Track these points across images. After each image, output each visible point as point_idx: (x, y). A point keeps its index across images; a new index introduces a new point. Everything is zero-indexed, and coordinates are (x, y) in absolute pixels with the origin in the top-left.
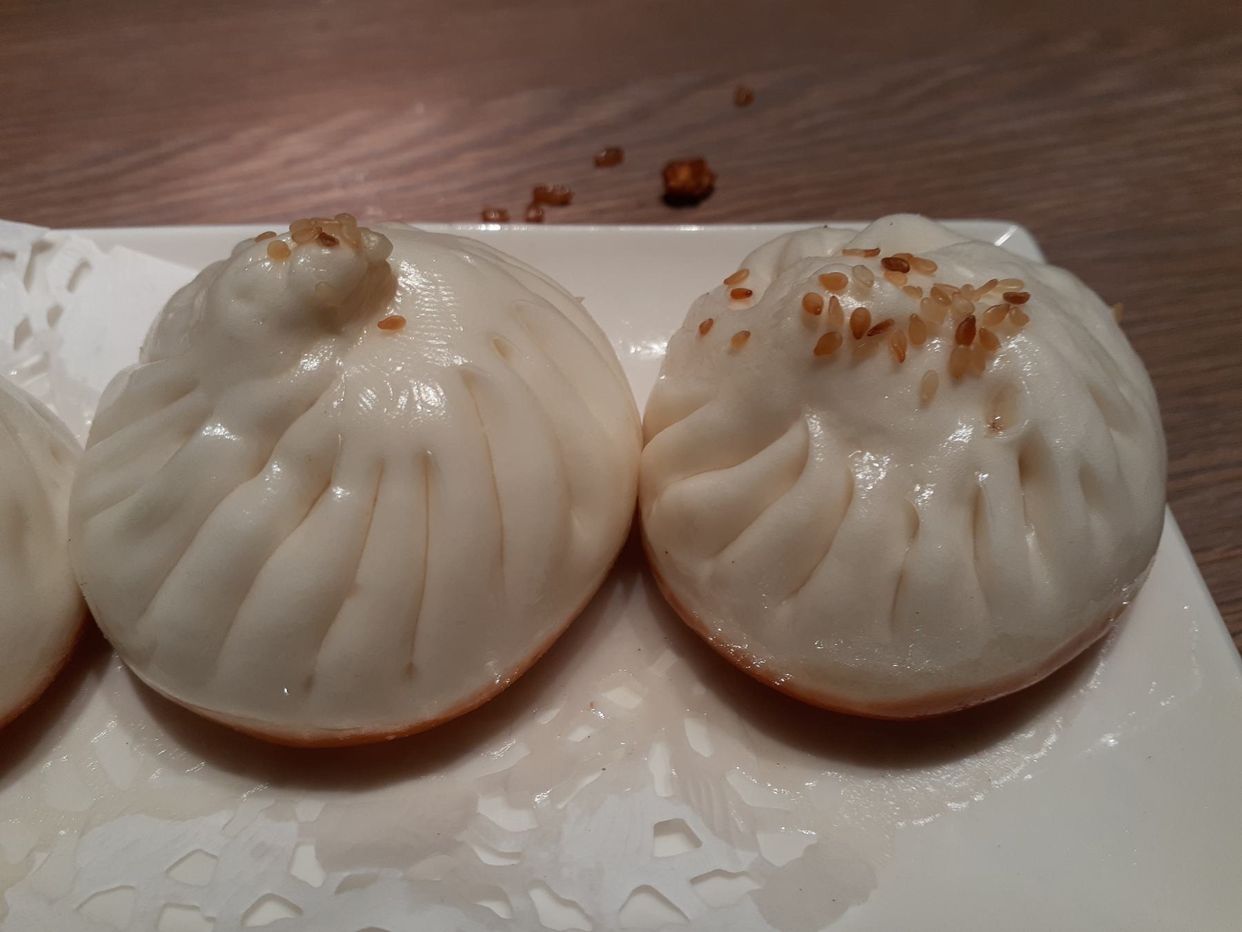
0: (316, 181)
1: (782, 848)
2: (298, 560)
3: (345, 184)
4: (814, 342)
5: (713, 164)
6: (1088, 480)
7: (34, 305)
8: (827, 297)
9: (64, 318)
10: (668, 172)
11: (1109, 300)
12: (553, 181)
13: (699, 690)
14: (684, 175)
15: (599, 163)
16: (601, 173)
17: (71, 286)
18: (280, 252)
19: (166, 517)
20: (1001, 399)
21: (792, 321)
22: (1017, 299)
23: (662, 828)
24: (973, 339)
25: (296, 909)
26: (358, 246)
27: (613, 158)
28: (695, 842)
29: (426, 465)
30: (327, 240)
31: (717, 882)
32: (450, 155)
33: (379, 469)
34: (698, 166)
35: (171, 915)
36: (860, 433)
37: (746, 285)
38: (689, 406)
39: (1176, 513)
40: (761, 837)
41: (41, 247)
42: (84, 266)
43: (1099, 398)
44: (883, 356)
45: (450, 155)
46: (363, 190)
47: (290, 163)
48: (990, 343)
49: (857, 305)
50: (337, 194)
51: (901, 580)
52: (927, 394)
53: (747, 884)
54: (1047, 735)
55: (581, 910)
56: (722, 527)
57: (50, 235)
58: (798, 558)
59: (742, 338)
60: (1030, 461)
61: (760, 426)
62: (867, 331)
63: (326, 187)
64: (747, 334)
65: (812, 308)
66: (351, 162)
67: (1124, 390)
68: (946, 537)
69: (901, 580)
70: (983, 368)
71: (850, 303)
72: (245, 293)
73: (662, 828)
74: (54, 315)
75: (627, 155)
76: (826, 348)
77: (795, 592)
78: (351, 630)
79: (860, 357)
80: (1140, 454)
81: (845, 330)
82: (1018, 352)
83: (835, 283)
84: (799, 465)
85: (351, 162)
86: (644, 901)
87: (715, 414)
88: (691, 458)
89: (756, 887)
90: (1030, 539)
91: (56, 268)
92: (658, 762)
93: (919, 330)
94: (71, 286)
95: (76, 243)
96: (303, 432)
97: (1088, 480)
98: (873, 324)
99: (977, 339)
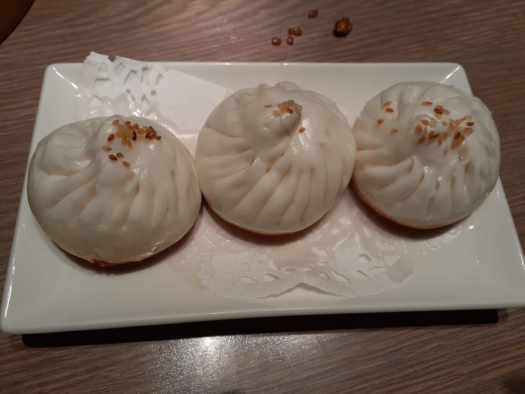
0: (210, 23)
1: (391, 261)
2: (281, 194)
3: (221, 25)
4: (419, 138)
5: (351, 20)
6: (482, 174)
7: (145, 89)
8: (424, 127)
9: (157, 94)
10: (337, 24)
11: (490, 110)
12: (294, 26)
13: (365, 218)
14: (343, 26)
15: (310, 17)
16: (311, 20)
17: (157, 81)
18: (276, 114)
19: (245, 184)
20: (463, 152)
21: (412, 132)
22: (470, 124)
23: (360, 256)
24: (459, 137)
25: (277, 278)
26: (297, 112)
27: (314, 14)
28: (369, 259)
29: (312, 170)
30: (290, 111)
31: (375, 269)
32: (256, 12)
33: (301, 171)
34: (347, 21)
35: (242, 278)
36: (426, 162)
37: (390, 107)
38: (375, 147)
39: (501, 179)
40: (386, 258)
41: (145, 69)
42: (160, 75)
43: (487, 149)
44: (436, 142)
45: (256, 12)
46: (228, 28)
47: (198, 14)
48: (463, 138)
49: (432, 129)
50: (218, 29)
51: (432, 200)
52: (445, 152)
53: (383, 270)
54: (457, 231)
55: (345, 277)
56: (385, 182)
57: (149, 64)
58: (406, 193)
59: (395, 131)
60: (468, 168)
61: (397, 157)
62: (433, 136)
63: (214, 26)
64: (397, 131)
65: (419, 130)
66: (220, 14)
67: (493, 144)
68: (445, 190)
69: (432, 200)
70: (460, 145)
71: (429, 129)
72: (267, 125)
73: (360, 256)
74: (154, 93)
75: (320, 13)
76: (421, 141)
77: (403, 200)
78: (293, 212)
79: (429, 143)
80: (495, 163)
81: (427, 136)
82: (469, 141)
83: (426, 123)
84: (410, 169)
85: (220, 14)
86: (359, 274)
87: (384, 151)
88: (376, 161)
89: (385, 270)
90: (465, 188)
91: (152, 76)
92: (357, 238)
93: (446, 135)
94: (157, 81)
95: (156, 67)
96: (281, 162)
97: (482, 174)
98: (435, 135)
99: (460, 137)
